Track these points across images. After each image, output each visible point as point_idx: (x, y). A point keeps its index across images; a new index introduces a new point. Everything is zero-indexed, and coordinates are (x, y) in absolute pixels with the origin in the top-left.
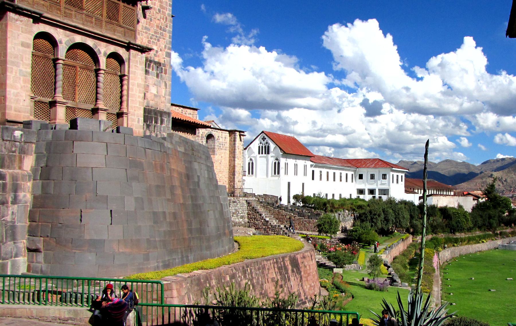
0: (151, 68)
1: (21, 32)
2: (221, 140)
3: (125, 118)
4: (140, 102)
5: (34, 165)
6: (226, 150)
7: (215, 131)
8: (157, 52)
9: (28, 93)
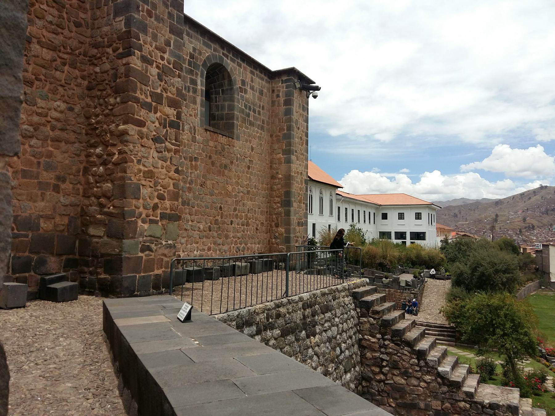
2: (249, 95)
7: (232, 60)
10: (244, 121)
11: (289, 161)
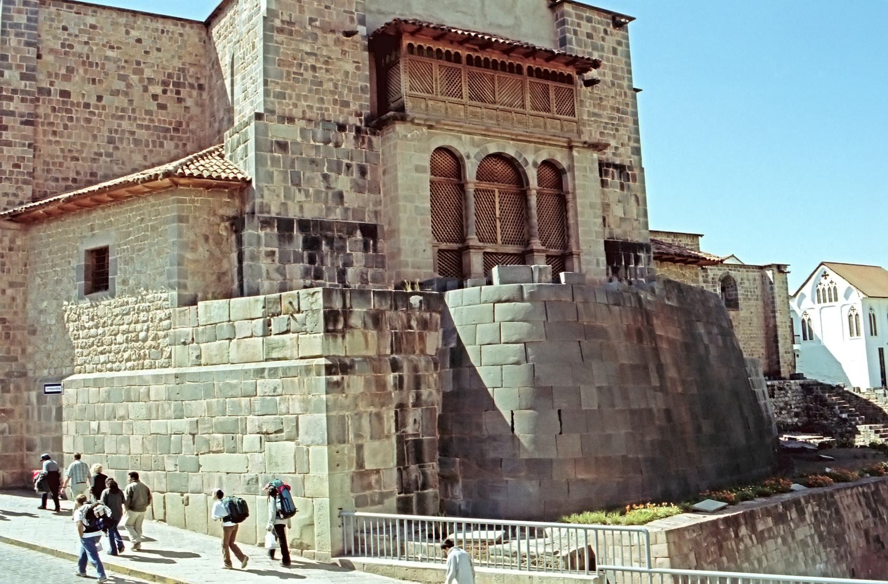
0: (610, 176)
1: (413, 153)
2: (747, 284)
3: (575, 260)
4: (596, 232)
5: (440, 346)
6: (757, 300)
7: (734, 270)
8: (616, 148)
9: (429, 239)
10: (744, 299)
11: (775, 317)
